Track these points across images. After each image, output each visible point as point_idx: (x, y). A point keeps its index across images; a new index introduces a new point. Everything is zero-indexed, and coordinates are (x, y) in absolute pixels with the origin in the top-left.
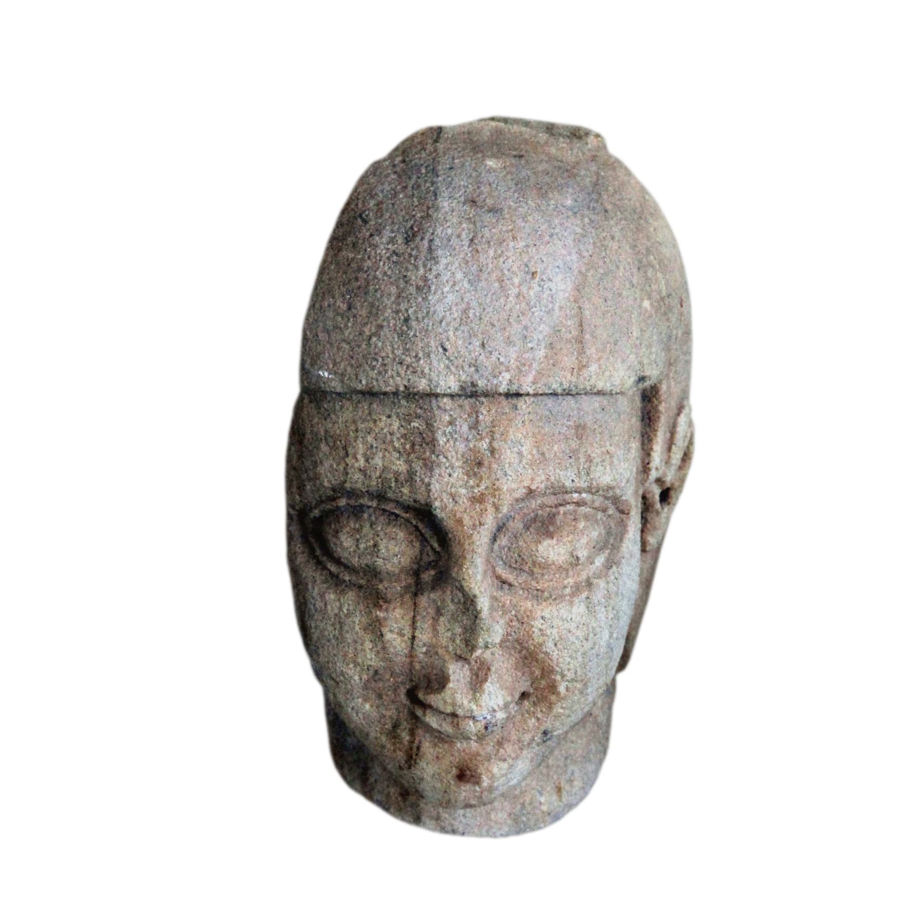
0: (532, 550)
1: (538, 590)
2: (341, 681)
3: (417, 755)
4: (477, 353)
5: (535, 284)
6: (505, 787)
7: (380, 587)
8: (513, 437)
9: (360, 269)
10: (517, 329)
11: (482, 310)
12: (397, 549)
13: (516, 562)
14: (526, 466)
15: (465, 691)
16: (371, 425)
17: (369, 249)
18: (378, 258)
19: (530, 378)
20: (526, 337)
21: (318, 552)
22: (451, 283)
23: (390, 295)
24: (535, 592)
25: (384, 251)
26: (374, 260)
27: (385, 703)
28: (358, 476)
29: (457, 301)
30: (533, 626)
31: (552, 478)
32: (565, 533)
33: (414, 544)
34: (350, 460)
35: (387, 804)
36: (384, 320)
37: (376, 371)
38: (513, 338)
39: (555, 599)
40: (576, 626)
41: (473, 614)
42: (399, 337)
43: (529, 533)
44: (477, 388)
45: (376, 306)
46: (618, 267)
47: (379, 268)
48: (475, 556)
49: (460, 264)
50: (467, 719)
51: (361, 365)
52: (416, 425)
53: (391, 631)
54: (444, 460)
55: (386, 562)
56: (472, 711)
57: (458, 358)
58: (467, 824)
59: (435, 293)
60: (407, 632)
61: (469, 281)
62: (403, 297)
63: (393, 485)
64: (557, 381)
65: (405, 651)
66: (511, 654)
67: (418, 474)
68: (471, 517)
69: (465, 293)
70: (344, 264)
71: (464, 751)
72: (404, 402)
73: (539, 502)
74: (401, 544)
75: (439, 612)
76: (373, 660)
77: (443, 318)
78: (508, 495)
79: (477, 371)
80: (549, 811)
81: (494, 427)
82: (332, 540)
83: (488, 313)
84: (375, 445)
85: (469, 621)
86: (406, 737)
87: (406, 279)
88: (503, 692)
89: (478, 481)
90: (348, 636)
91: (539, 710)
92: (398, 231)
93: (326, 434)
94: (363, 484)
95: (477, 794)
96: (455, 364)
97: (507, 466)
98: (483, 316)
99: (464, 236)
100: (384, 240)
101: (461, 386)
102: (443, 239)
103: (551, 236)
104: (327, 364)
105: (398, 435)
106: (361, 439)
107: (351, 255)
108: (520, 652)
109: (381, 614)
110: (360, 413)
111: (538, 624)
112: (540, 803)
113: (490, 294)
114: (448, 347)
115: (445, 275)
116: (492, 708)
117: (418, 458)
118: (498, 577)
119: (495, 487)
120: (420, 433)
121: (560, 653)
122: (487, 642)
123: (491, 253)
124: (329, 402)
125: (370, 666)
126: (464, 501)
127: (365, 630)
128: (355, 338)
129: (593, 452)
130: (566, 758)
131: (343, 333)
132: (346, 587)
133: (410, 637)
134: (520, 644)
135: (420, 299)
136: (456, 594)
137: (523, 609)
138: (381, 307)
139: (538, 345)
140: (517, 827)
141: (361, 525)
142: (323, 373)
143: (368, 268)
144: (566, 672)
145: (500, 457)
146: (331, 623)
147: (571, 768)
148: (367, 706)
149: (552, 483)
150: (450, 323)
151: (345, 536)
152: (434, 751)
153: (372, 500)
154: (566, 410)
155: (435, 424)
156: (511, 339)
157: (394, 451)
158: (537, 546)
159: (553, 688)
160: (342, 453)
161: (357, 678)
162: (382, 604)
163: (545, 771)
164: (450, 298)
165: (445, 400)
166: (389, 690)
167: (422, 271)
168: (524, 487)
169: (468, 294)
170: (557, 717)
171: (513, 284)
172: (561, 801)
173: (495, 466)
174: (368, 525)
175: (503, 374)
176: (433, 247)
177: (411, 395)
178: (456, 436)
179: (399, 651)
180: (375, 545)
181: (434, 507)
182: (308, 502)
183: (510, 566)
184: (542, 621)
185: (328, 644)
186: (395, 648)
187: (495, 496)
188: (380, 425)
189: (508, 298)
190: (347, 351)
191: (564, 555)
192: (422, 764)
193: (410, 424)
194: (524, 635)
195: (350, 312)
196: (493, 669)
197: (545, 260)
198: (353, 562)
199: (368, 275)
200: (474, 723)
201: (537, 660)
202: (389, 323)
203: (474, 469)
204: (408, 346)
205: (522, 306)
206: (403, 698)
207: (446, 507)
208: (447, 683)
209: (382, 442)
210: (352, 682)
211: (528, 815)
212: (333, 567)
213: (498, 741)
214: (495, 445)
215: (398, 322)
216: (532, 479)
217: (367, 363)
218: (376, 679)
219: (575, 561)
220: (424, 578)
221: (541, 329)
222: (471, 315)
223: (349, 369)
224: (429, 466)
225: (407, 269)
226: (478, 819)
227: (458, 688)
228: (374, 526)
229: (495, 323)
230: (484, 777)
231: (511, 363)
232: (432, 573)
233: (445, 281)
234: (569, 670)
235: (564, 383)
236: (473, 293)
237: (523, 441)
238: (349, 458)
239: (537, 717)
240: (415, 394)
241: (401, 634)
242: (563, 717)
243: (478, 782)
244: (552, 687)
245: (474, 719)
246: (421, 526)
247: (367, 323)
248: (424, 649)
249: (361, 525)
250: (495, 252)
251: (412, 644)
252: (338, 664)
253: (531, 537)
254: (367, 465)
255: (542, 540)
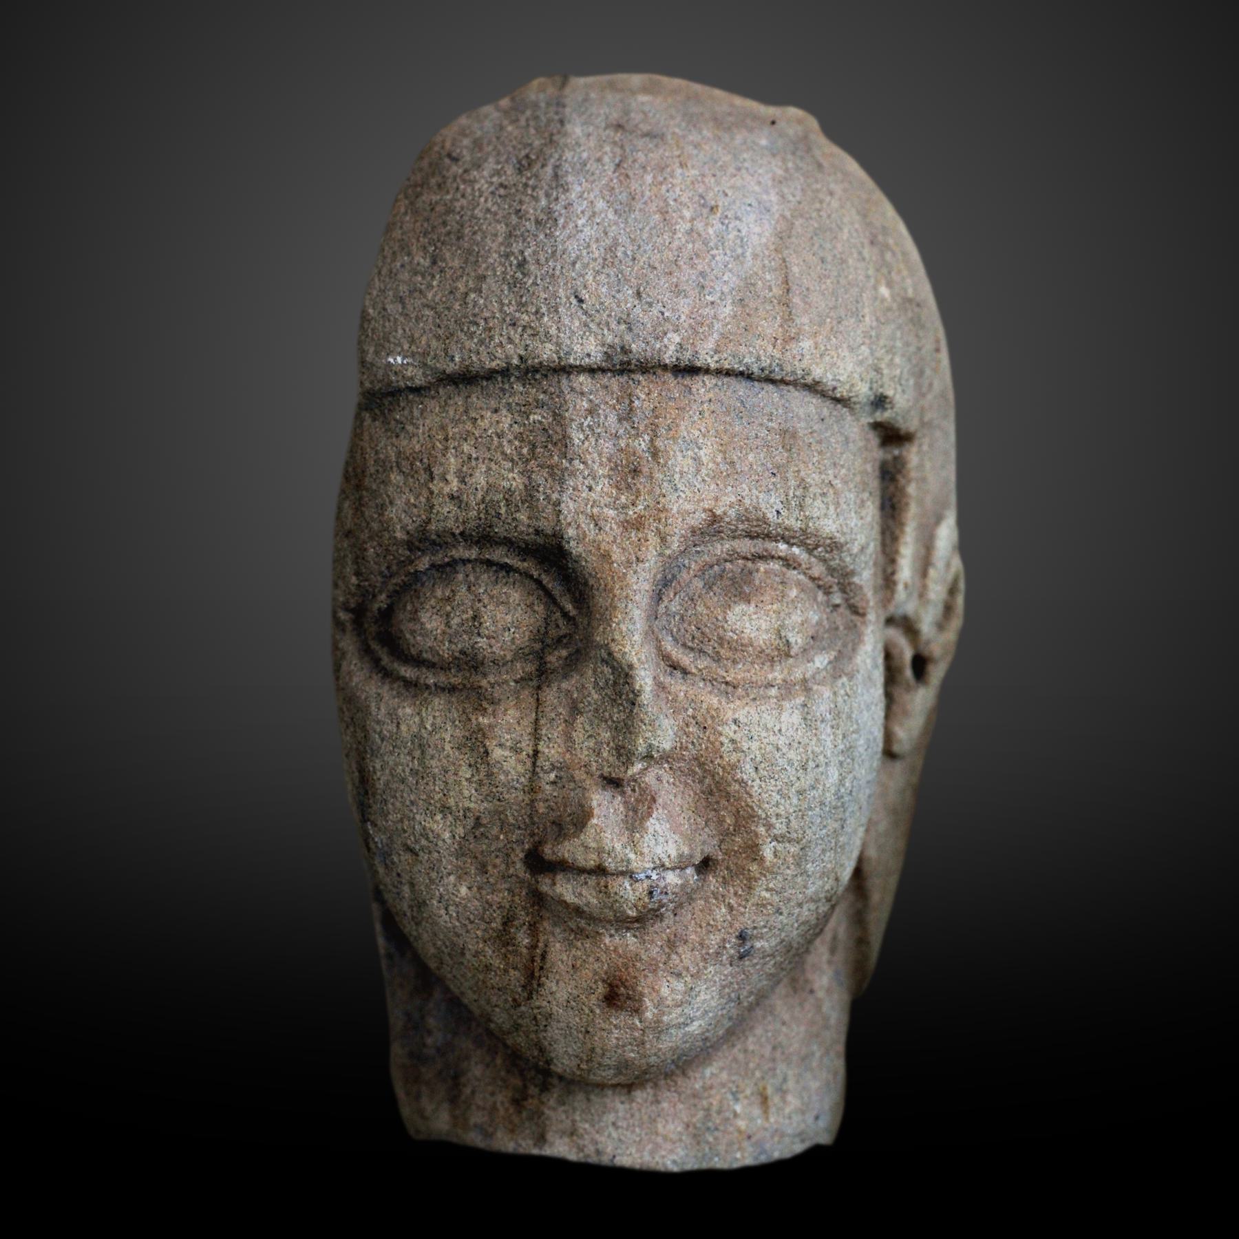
0: (717, 619)
1: (727, 683)
2: (422, 849)
3: (542, 968)
4: (629, 305)
5: (715, 220)
6: (681, 1033)
7: (484, 683)
8: (686, 434)
9: (450, 211)
10: (689, 274)
11: (636, 248)
12: (509, 618)
13: (693, 638)
14: (706, 478)
15: (617, 830)
16: (469, 426)
17: (462, 187)
18: (477, 194)
19: (710, 344)
20: (703, 287)
21: (386, 660)
22: (587, 215)
23: (496, 235)
24: (723, 685)
25: (486, 186)
26: (470, 198)
27: (491, 880)
28: (448, 508)
29: (598, 235)
30: (721, 734)
31: (747, 501)
32: (767, 598)
33: (536, 608)
34: (436, 486)
35: (490, 1126)
36: (487, 269)
37: (476, 340)
38: (683, 287)
39: (754, 699)
40: (787, 742)
41: (627, 700)
42: (510, 288)
43: (712, 594)
44: (631, 356)
45: (475, 254)
46: (841, 229)
47: (478, 205)
48: (630, 605)
49: (601, 192)
50: (621, 878)
51: (452, 335)
52: (536, 417)
53: (501, 745)
54: (582, 467)
55: (493, 641)
56: (628, 861)
57: (602, 312)
58: (620, 1140)
59: (564, 227)
60: (527, 746)
61: (616, 212)
62: (515, 236)
63: (503, 511)
64: (750, 352)
65: (522, 779)
66: (686, 784)
67: (541, 489)
68: (623, 549)
69: (609, 225)
70: (425, 210)
71: (615, 950)
72: (518, 387)
73: (727, 546)
74: (516, 609)
75: (575, 710)
76: (473, 799)
77: (578, 258)
78: (680, 519)
79: (630, 329)
80: (750, 1132)
81: (657, 417)
82: (407, 627)
83: (645, 251)
84: (474, 456)
85: (622, 714)
86: (524, 940)
87: (520, 214)
88: (676, 837)
89: (634, 497)
90: (434, 763)
91: (732, 891)
92: (507, 161)
93: (398, 458)
94: (457, 520)
95: (636, 1034)
96: (597, 320)
97: (677, 476)
98: (638, 256)
99: (606, 159)
100: (485, 173)
101: (606, 353)
102: (575, 164)
103: (739, 169)
104: (400, 345)
105: (511, 437)
106: (453, 451)
107: (435, 198)
108: (701, 782)
109: (485, 721)
110: (451, 413)
111: (729, 731)
112: (736, 1115)
113: (647, 228)
114: (584, 295)
115: (581, 205)
116: (660, 859)
117: (541, 466)
118: (666, 657)
119: (660, 506)
120: (544, 429)
121: (763, 785)
122: (650, 745)
123: (649, 178)
124: (403, 409)
125: (469, 809)
126: (612, 528)
127: (458, 748)
128: (444, 299)
129: (808, 475)
130: (774, 1048)
131: (425, 297)
132: (430, 694)
133: (531, 753)
134: (701, 765)
135: (542, 236)
136: (602, 672)
137: (705, 706)
138: (482, 252)
139: (722, 300)
140: (698, 1151)
141: (452, 591)
142: (395, 359)
143: (462, 208)
144: (773, 820)
145: (667, 462)
146: (406, 751)
147: (781, 1067)
148: (464, 890)
149: (746, 510)
150: (588, 264)
151: (428, 615)
152: (568, 957)
153: (470, 548)
154: (766, 405)
155: (567, 415)
156: (681, 288)
157: (504, 460)
158: (725, 612)
159: (753, 850)
160: (423, 477)
161: (447, 835)
162: (487, 706)
163: (741, 1056)
164: (588, 232)
165: (582, 378)
166: (497, 857)
167: (543, 202)
168: (705, 510)
169: (614, 228)
170: (762, 905)
171: (682, 218)
172: (767, 1119)
173: (658, 476)
174: (464, 589)
175: (669, 335)
176: (560, 173)
177: (532, 372)
178: (599, 430)
179: (513, 780)
180: (475, 618)
181: (566, 536)
182: (370, 585)
183: (684, 645)
184: (734, 727)
185: (402, 787)
186: (507, 773)
187: (660, 520)
188: (482, 424)
189: (675, 234)
190: (430, 320)
191: (767, 631)
192: (551, 985)
193: (528, 418)
194: (707, 748)
195: (435, 268)
196: (660, 801)
197: (730, 194)
198: (441, 653)
199: (462, 217)
200: (631, 885)
201: (728, 796)
202: (494, 270)
203: (626, 480)
204: (524, 299)
205: (696, 246)
206: (519, 868)
207: (585, 536)
208: (589, 819)
209: (485, 449)
210: (440, 843)
211: (716, 1133)
212: (409, 671)
213: (669, 941)
214: (659, 443)
215: (509, 268)
216: (716, 499)
217: (462, 330)
218: (477, 833)
219: (784, 652)
220: (550, 662)
221: (726, 278)
222: (619, 254)
223: (434, 343)
224: (558, 476)
225: (521, 202)
226: (637, 1130)
227: (607, 826)
228: (473, 588)
229: (657, 265)
230: (648, 1002)
231: (681, 321)
232: (564, 653)
233: (579, 212)
234: (778, 815)
235: (763, 358)
236: (622, 225)
237: (701, 441)
238: (435, 482)
239: (729, 903)
240: (536, 371)
241: (516, 750)
242: (769, 907)
243: (637, 1011)
244: (751, 847)
245: (631, 877)
246: (545, 579)
247: (462, 276)
248: (552, 776)
249: (452, 591)
250: (654, 177)
251: (534, 764)
252: (418, 817)
253: (716, 599)
254: (463, 486)
255: (732, 604)
